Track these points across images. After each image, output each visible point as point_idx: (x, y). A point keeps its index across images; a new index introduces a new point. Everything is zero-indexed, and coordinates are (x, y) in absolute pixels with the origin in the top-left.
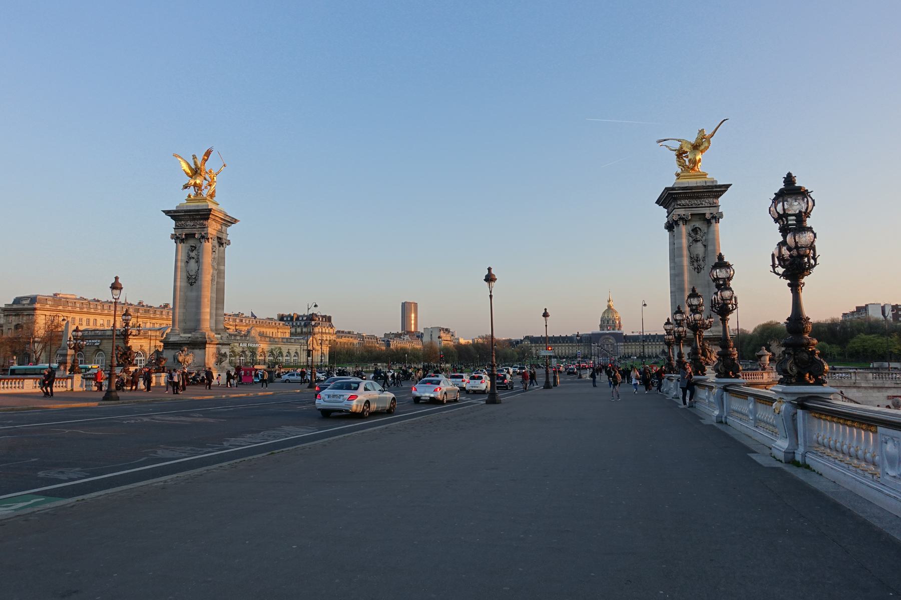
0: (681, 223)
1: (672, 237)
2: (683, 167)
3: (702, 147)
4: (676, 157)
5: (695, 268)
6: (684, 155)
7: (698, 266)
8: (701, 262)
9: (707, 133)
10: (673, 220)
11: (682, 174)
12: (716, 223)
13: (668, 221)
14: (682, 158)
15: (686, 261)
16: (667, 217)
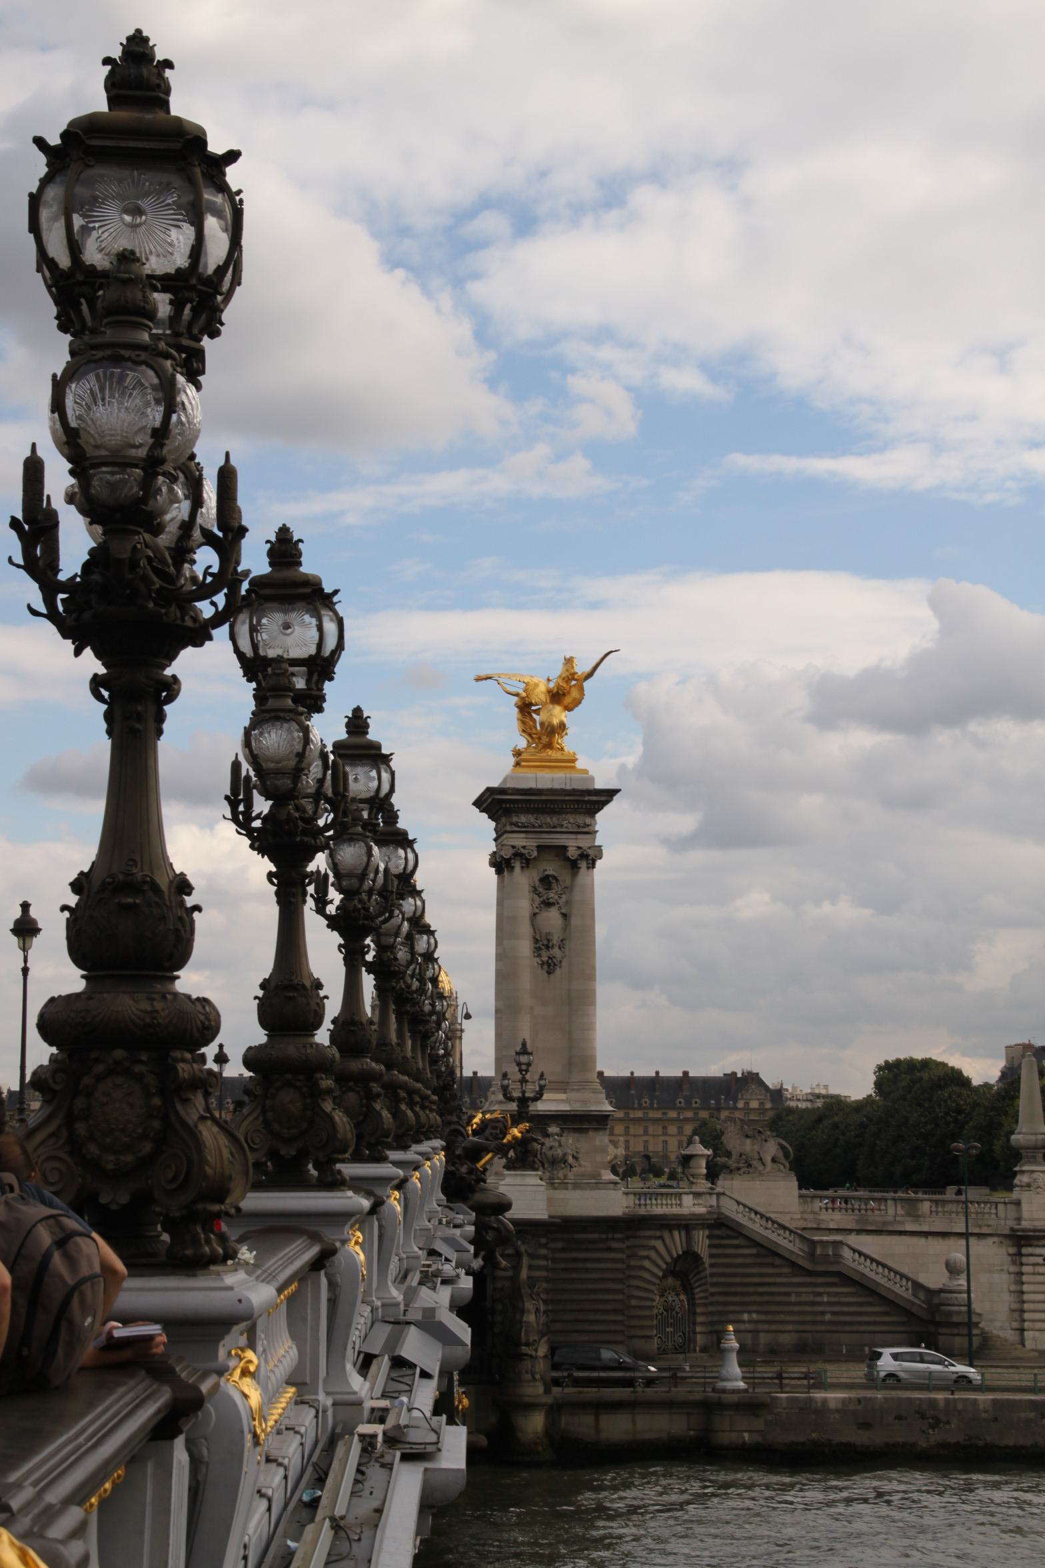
0: (517, 865)
1: (501, 887)
2: (530, 735)
3: (567, 700)
4: (516, 710)
5: (543, 964)
6: (533, 708)
7: (549, 957)
8: (556, 952)
9: (581, 668)
10: (502, 857)
11: (524, 756)
12: (588, 868)
13: (494, 853)
14: (529, 714)
15: (525, 948)
16: (495, 840)
